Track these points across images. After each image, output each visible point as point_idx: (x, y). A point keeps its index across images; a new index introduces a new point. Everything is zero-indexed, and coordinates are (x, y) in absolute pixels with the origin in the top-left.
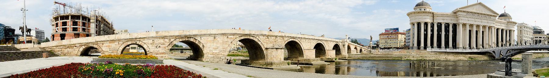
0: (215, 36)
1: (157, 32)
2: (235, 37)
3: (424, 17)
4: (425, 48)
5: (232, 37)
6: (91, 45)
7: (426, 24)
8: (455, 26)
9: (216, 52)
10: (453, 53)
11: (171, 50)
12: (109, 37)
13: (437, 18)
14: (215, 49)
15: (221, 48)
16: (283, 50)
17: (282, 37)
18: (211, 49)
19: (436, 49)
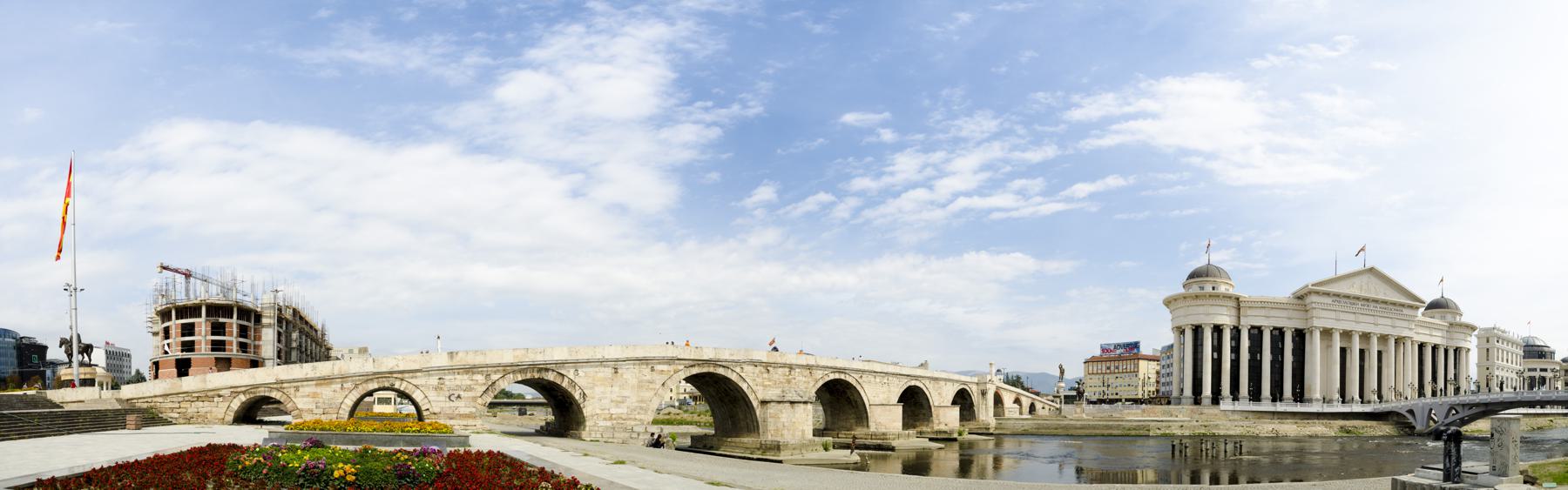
0: (616, 365)
1: (451, 354)
2: (672, 368)
3: (1212, 310)
4: (1216, 398)
5: (665, 367)
6: (262, 392)
7: (1218, 330)
8: (1300, 336)
9: (619, 411)
10: (1294, 414)
11: (492, 405)
12: (314, 368)
13: (1249, 312)
14: (618, 403)
15: (633, 401)
16: (810, 407)
17: (809, 367)
18: (606, 402)
19: (1245, 405)
